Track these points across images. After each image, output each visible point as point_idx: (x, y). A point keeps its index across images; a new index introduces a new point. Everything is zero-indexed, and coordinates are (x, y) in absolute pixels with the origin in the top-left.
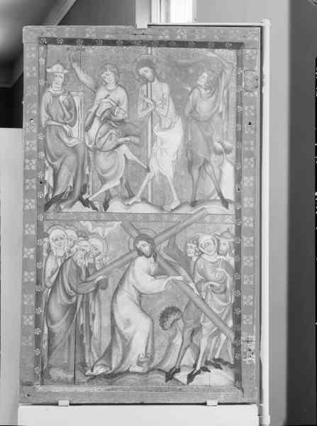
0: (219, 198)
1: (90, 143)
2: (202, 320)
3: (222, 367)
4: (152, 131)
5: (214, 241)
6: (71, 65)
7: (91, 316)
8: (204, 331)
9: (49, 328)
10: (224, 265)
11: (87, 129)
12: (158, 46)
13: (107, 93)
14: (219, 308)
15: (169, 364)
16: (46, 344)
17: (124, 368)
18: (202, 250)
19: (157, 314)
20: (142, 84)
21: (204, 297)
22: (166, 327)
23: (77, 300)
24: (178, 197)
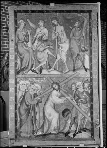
0: (84, 68)
1: (34, 48)
3: (86, 131)
4: (58, 44)
5: (82, 84)
6: (27, 21)
8: (79, 118)
11: (33, 43)
12: (59, 12)
13: (40, 30)
15: (66, 130)
16: (19, 123)
17: (49, 132)
18: (77, 87)
20: (53, 27)
21: (79, 105)
22: (64, 116)
23: (30, 107)
24: (68, 68)
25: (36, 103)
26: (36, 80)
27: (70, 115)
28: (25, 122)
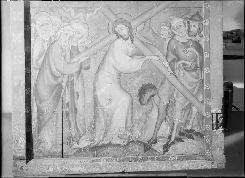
2: (175, 96)
3: (195, 137)
7: (75, 95)
9: (38, 107)
10: (195, 45)
14: (191, 84)
15: (147, 136)
16: (36, 121)
17: (106, 141)
19: (135, 92)
21: (177, 75)
22: (143, 102)
25: (77, 69)
26: (76, 12)
27: (156, 98)
28: (50, 118)
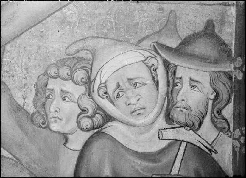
5: (152, 70)
